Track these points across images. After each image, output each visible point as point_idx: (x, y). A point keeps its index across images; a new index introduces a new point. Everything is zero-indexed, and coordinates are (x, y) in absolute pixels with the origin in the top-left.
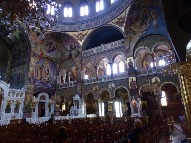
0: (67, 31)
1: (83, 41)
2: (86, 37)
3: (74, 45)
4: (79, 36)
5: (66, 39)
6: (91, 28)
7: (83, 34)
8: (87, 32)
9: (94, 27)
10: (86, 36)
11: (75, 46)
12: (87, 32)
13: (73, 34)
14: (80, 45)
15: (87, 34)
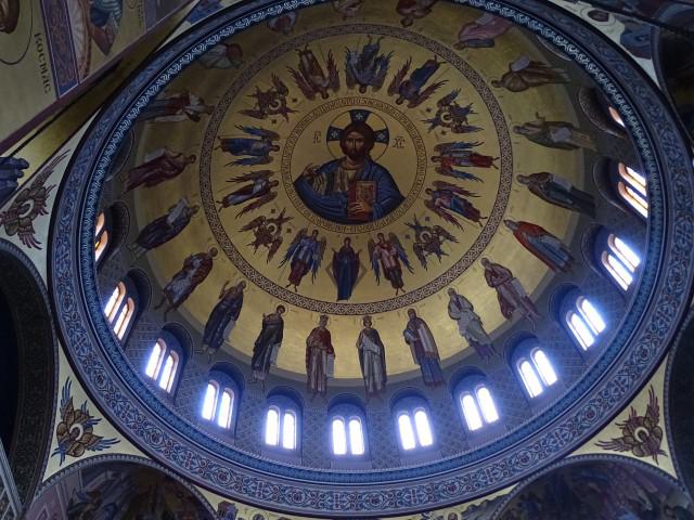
0: (568, 446)
1: (664, 446)
2: (662, 418)
3: (641, 493)
4: (633, 437)
5: (592, 485)
6: (651, 364)
7: (641, 413)
8: (652, 393)
9: (660, 350)
10: (661, 412)
11: (650, 496)
12: (652, 393)
13: (606, 446)
14: (671, 477)
15: (661, 404)
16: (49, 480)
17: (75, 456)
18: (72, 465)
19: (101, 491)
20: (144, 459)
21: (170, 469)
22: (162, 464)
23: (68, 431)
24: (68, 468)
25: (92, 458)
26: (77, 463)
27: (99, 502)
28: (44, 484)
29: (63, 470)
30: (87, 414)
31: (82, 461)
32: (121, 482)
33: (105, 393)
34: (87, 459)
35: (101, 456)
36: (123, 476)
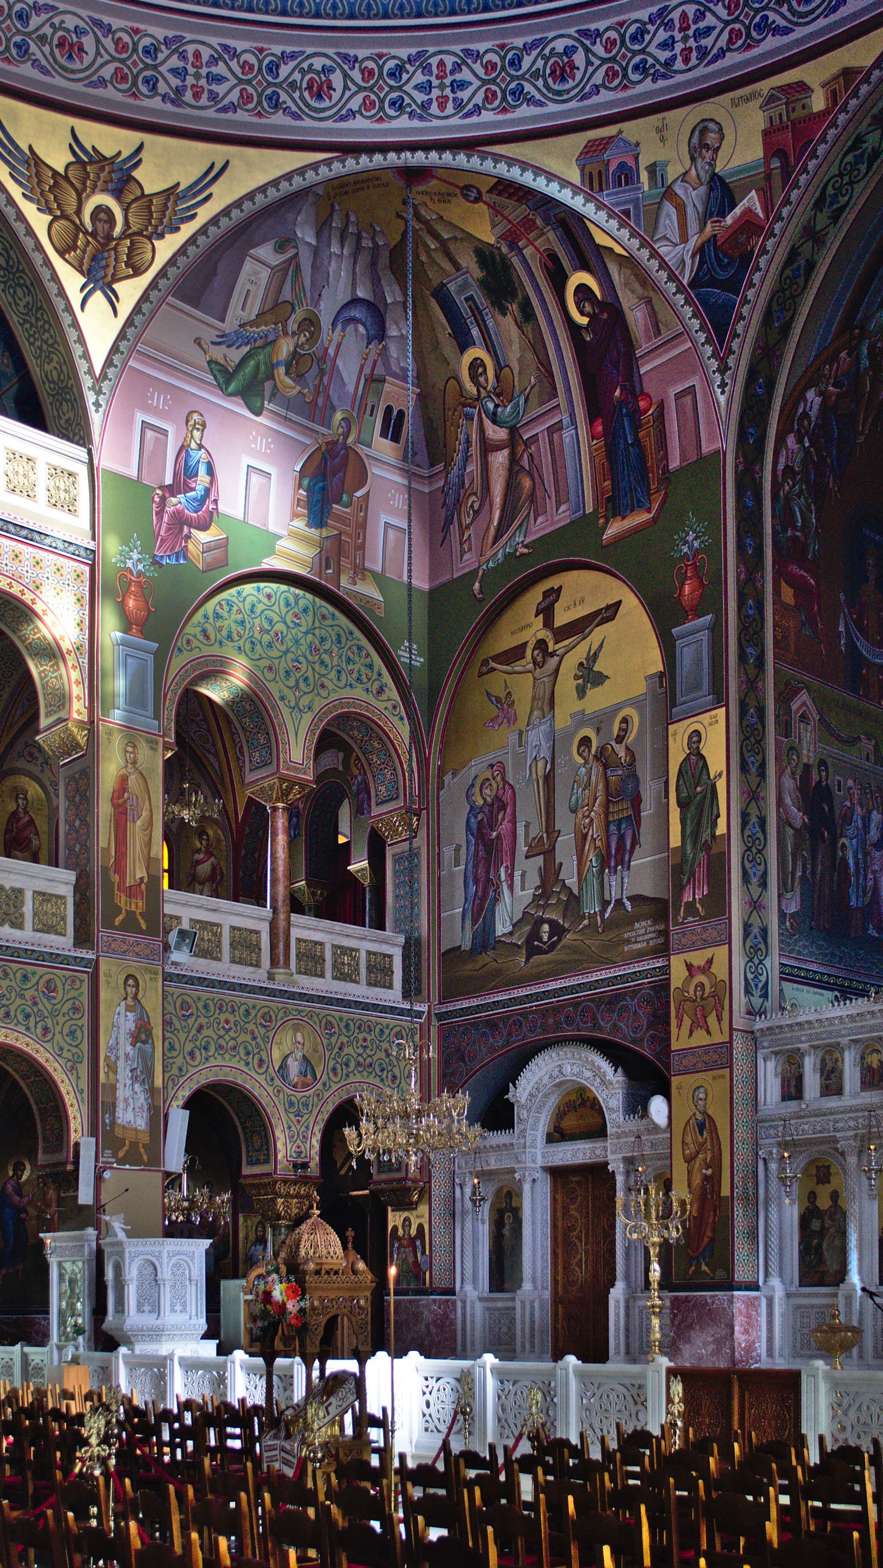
16: (109, 363)
17: (138, 272)
18: (145, 297)
19: (287, 294)
20: (315, 166)
21: (399, 148)
22: (371, 149)
23: (79, 228)
24: (137, 309)
25: (182, 251)
26: (153, 285)
27: (311, 323)
28: (104, 376)
29: (129, 322)
30: (99, 159)
31: (162, 273)
32: (316, 252)
33: (107, 72)
34: (172, 261)
35: (203, 230)
36: (306, 235)
